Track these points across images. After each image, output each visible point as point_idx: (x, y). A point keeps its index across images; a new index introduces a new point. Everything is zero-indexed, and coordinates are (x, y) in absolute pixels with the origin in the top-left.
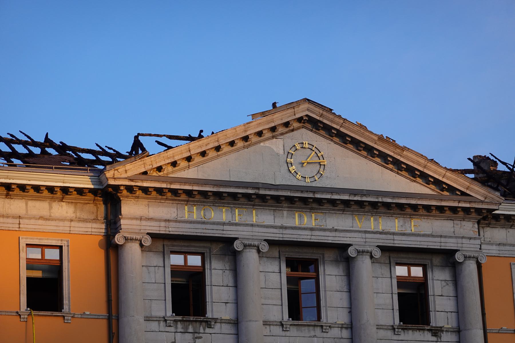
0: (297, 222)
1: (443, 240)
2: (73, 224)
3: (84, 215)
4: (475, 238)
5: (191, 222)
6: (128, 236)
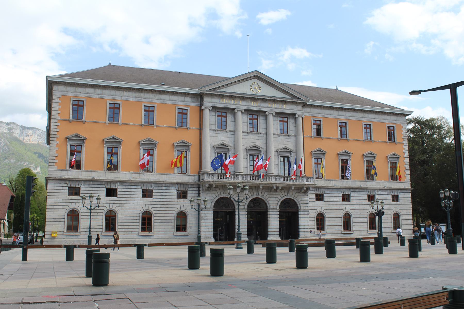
0: (252, 104)
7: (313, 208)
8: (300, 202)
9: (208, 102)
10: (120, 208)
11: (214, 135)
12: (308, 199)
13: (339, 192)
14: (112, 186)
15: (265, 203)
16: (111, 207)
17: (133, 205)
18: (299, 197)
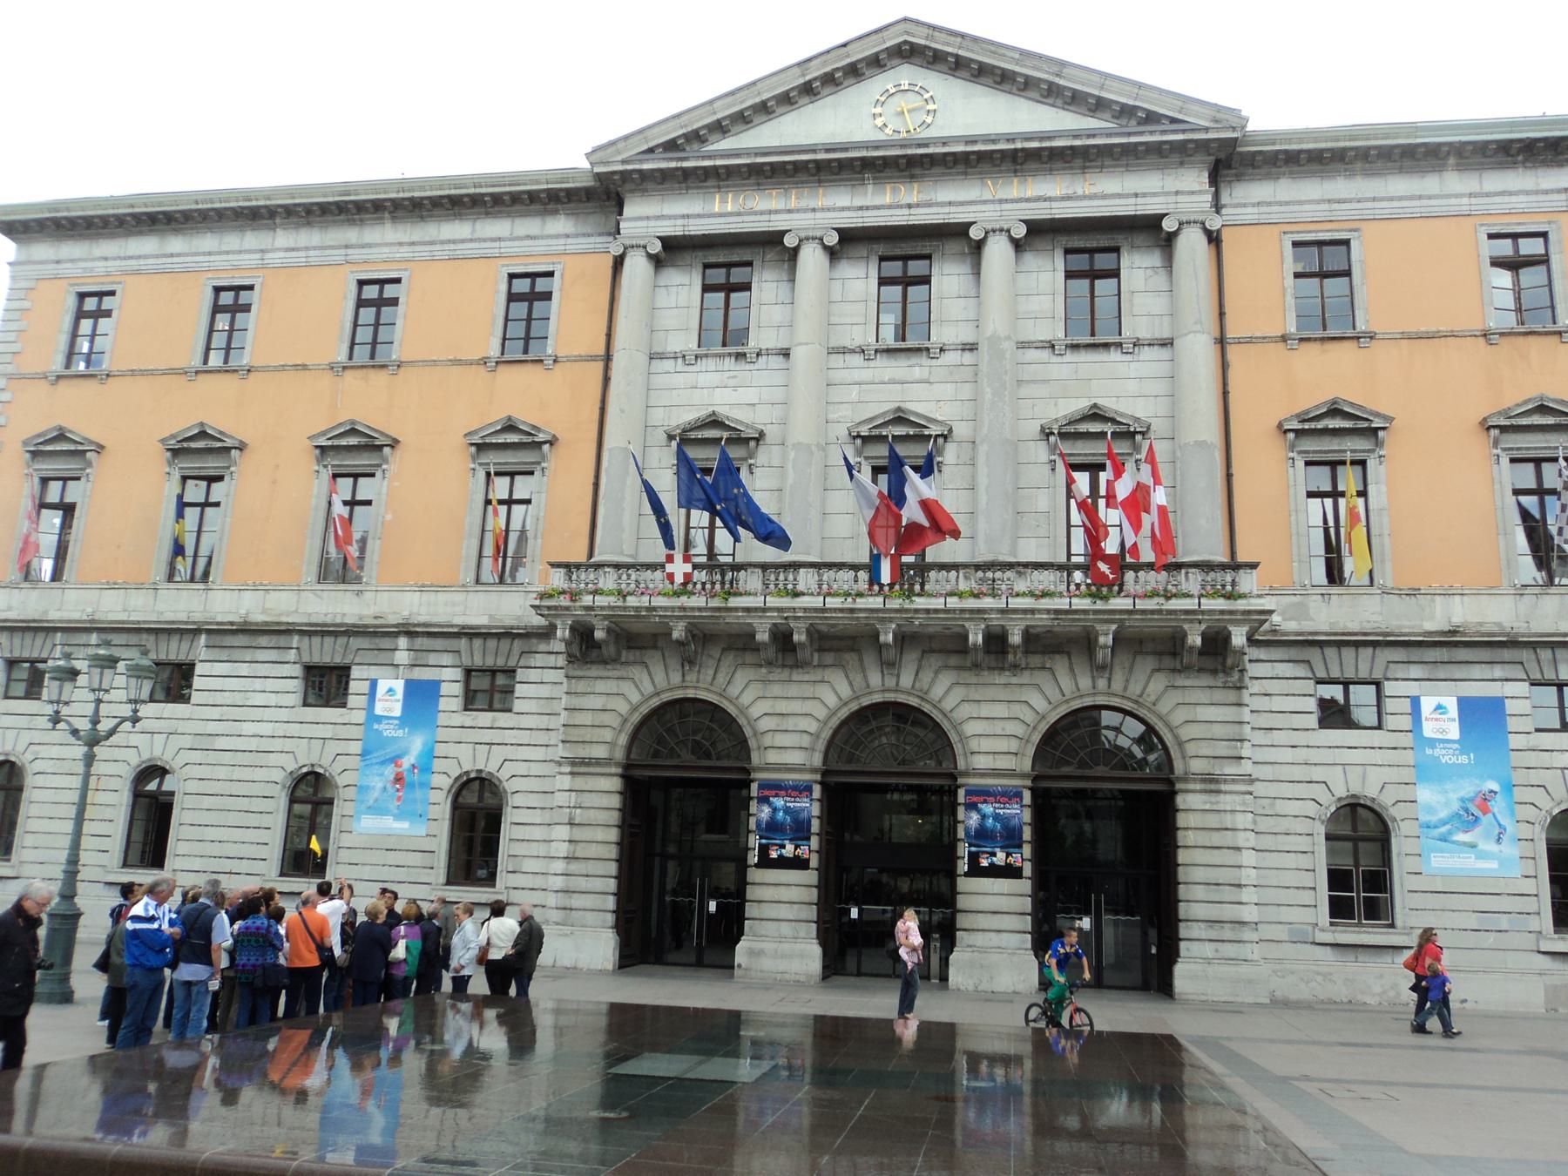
1: (1139, 200)
2: (570, 241)
3: (581, 229)
4: (1200, 192)
5: (721, 215)
6: (628, 242)
7: (1298, 773)
8: (1186, 733)
9: (650, 218)
10: (197, 756)
11: (679, 380)
12: (1246, 714)
13: (1498, 672)
14: (174, 651)
15: (943, 734)
16: (157, 753)
17: (253, 744)
18: (1173, 697)
